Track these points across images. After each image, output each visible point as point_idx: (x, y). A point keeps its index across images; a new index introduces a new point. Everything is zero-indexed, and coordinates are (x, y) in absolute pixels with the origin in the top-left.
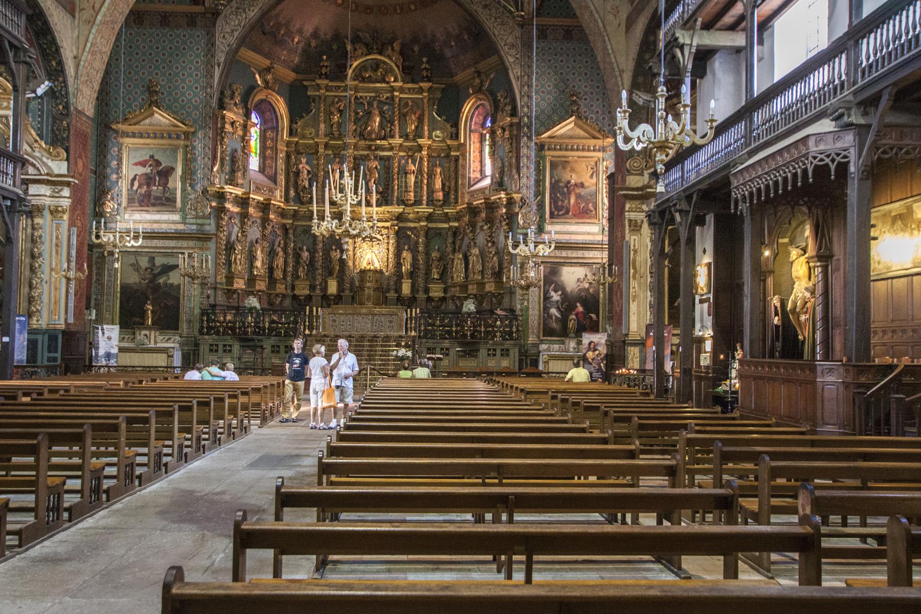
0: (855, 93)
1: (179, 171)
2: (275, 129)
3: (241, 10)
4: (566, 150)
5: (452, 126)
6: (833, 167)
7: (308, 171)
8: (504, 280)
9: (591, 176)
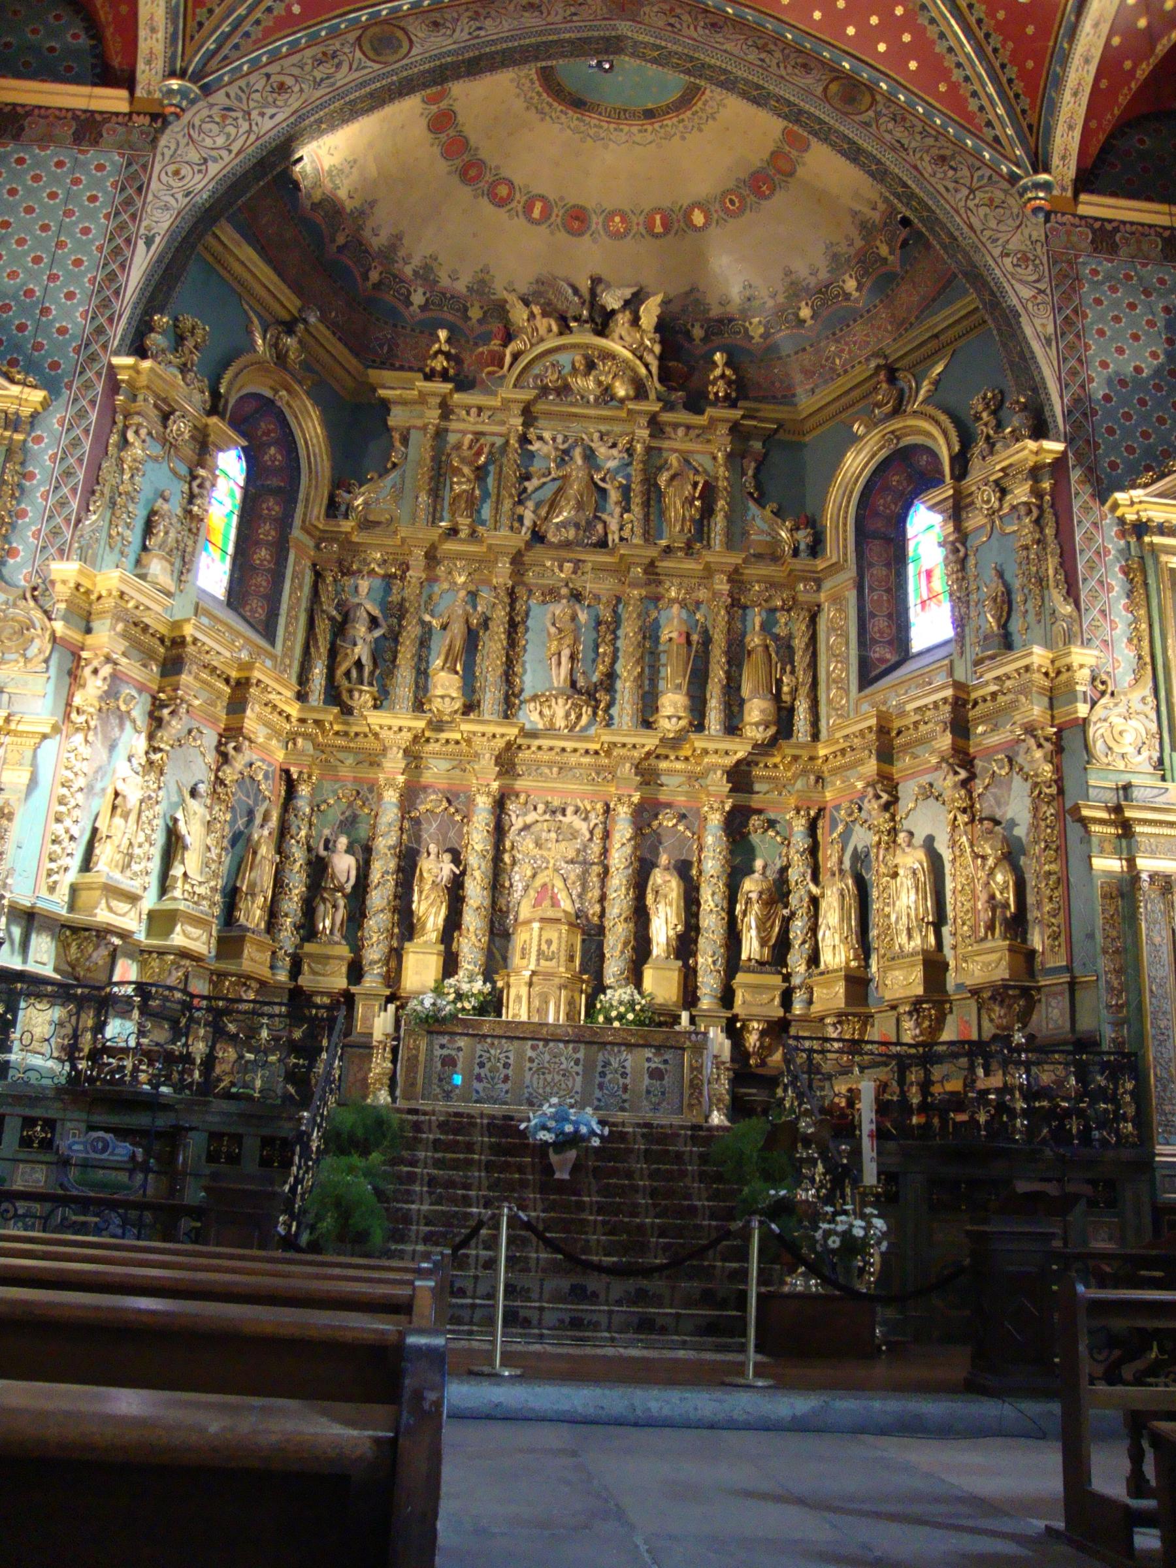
2: (289, 496)
3: (239, 114)
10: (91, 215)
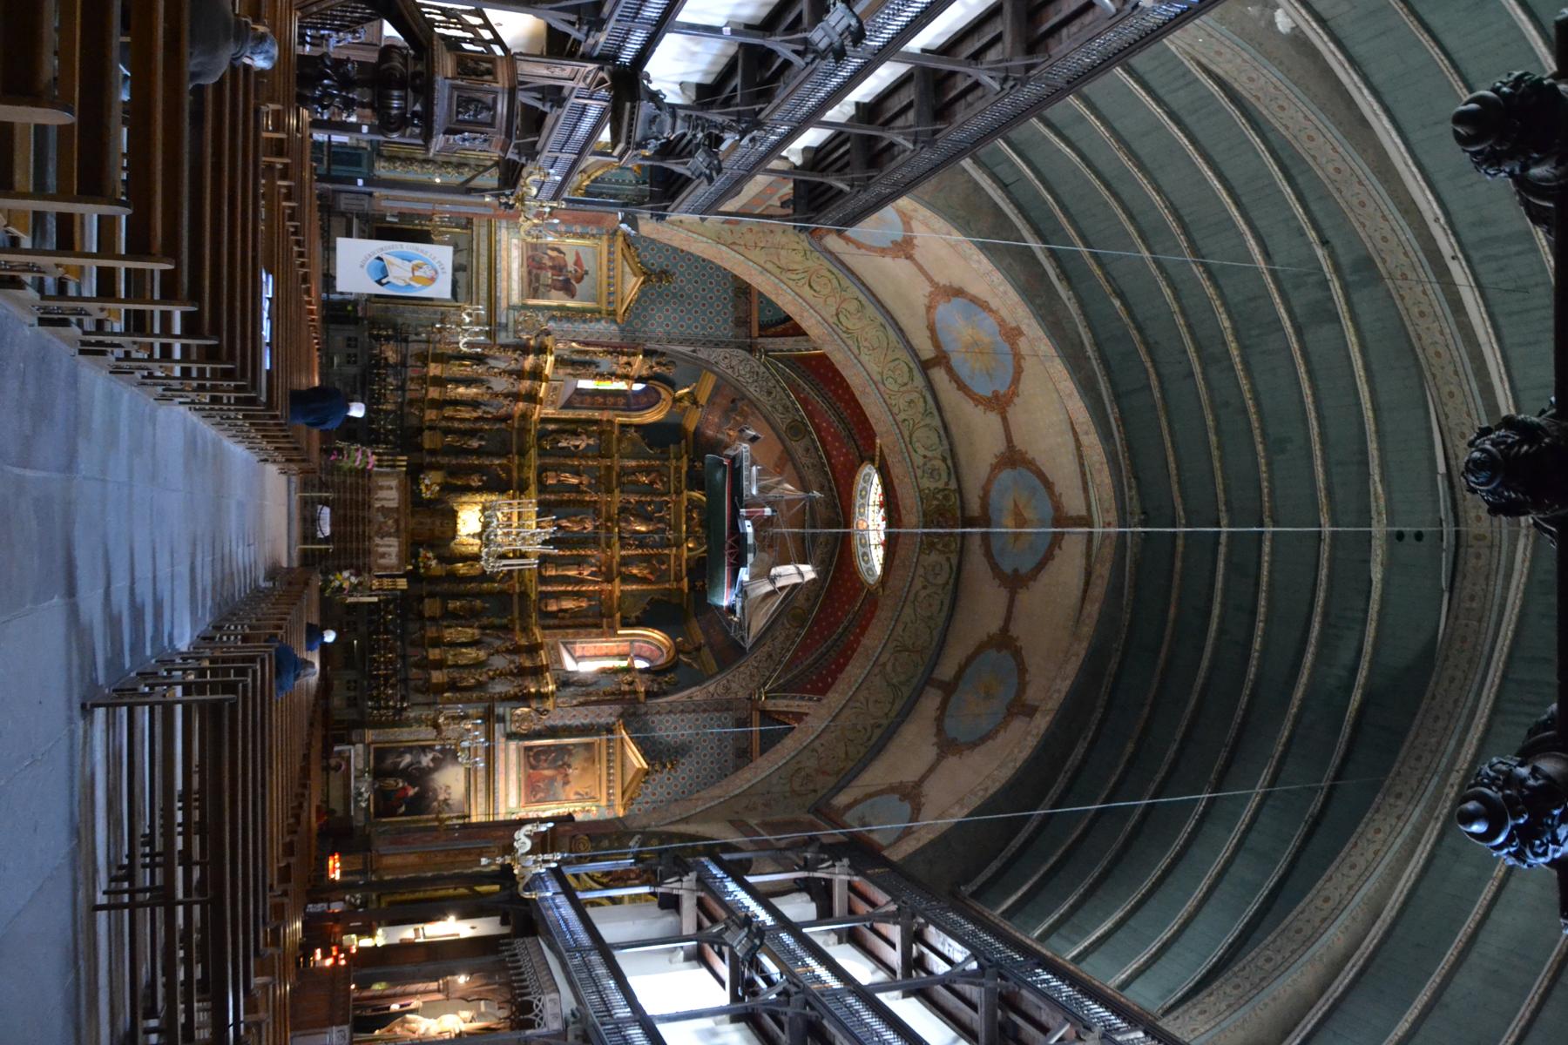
0: (594, 1025)
1: (570, 304)
4: (609, 761)
5: (637, 617)
6: (530, 1016)
7: (577, 447)
8: (446, 695)
9: (577, 793)
10: (703, 328)
